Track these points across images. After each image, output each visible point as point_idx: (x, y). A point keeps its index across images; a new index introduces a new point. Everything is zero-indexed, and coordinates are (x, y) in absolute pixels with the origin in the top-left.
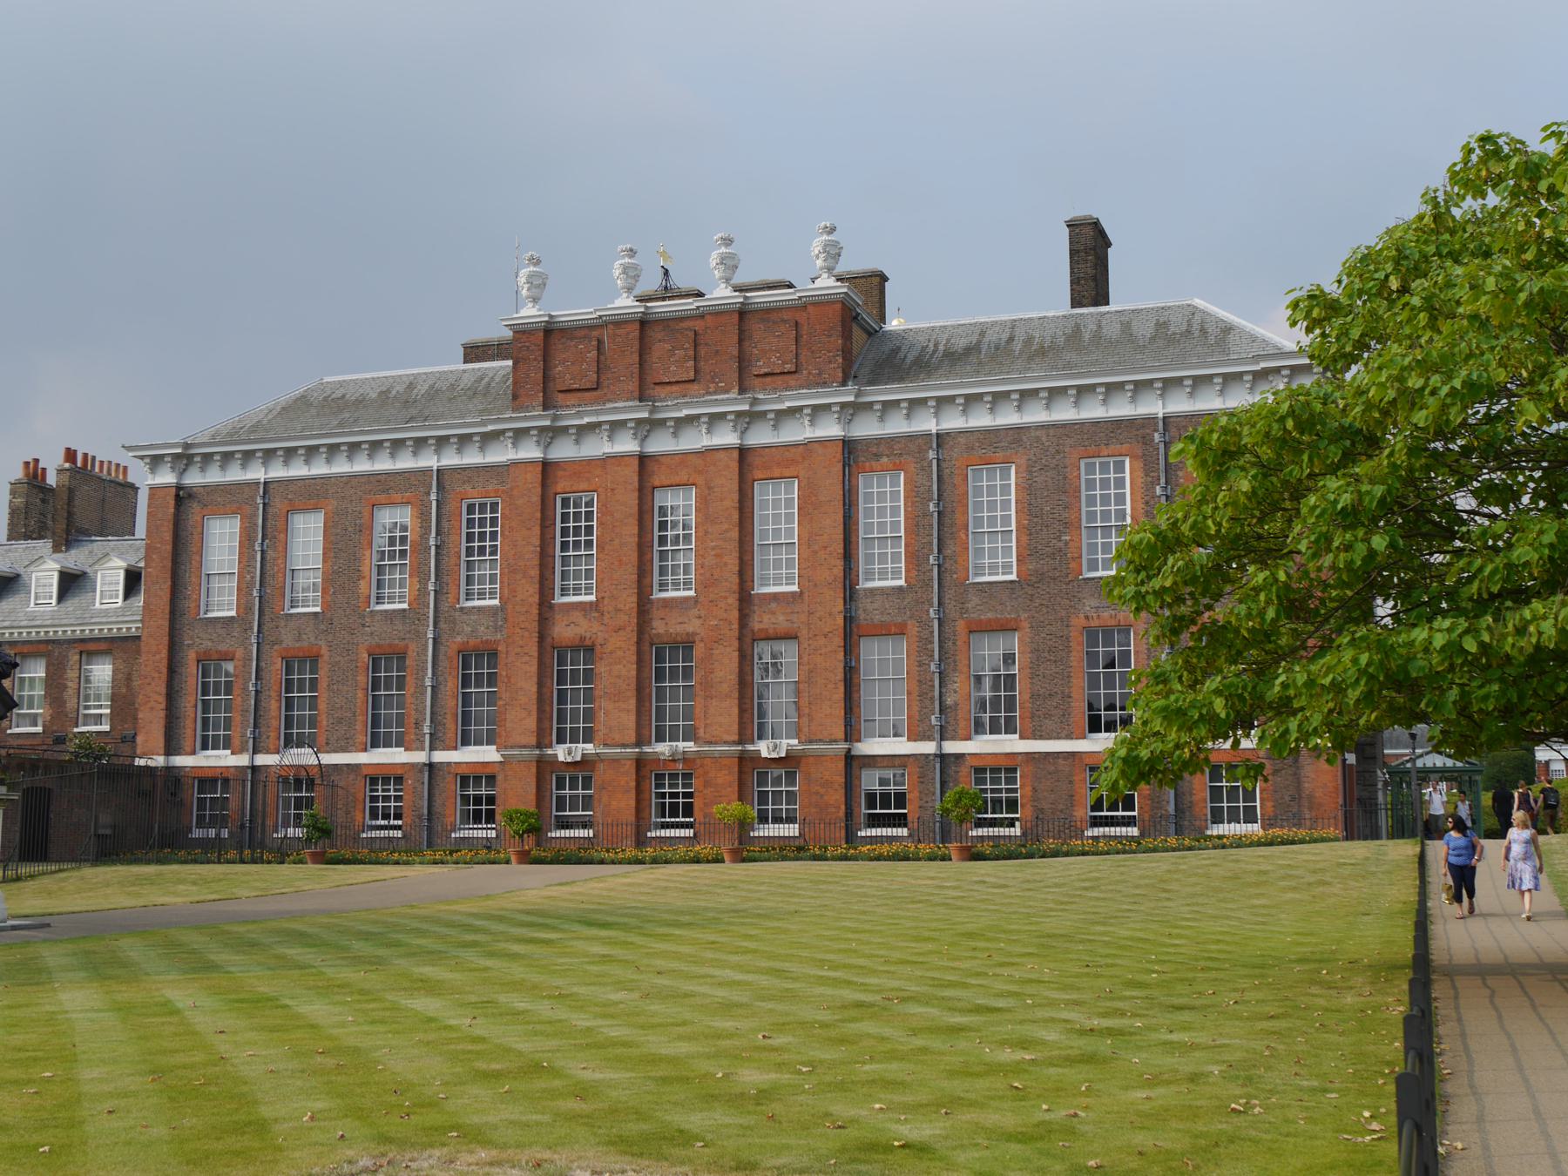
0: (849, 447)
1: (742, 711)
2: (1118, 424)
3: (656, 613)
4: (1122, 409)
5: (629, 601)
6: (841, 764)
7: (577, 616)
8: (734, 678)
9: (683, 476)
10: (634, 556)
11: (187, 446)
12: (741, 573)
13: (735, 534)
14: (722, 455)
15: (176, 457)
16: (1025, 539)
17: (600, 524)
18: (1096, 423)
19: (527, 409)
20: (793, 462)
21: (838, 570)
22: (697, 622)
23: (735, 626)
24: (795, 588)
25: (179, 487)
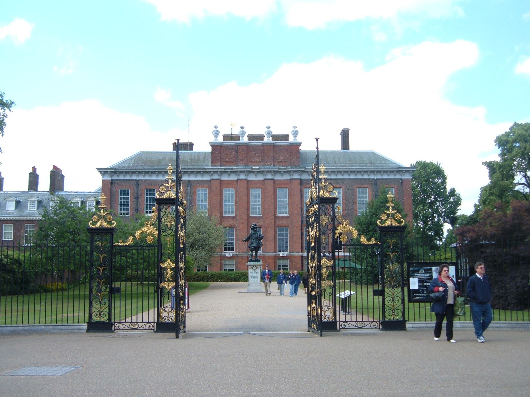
0: (301, 182)
1: (275, 245)
2: (365, 180)
3: (250, 220)
4: (366, 177)
5: (245, 217)
6: (301, 258)
7: (230, 220)
8: (273, 236)
9: (258, 185)
10: (246, 205)
11: (116, 169)
12: (274, 210)
13: (273, 201)
14: (269, 181)
15: (111, 172)
16: (344, 206)
17: (236, 196)
18: (360, 180)
19: (216, 166)
20: (287, 184)
21: (300, 211)
22: (262, 222)
23: (273, 224)
24: (287, 215)
25: (111, 180)
